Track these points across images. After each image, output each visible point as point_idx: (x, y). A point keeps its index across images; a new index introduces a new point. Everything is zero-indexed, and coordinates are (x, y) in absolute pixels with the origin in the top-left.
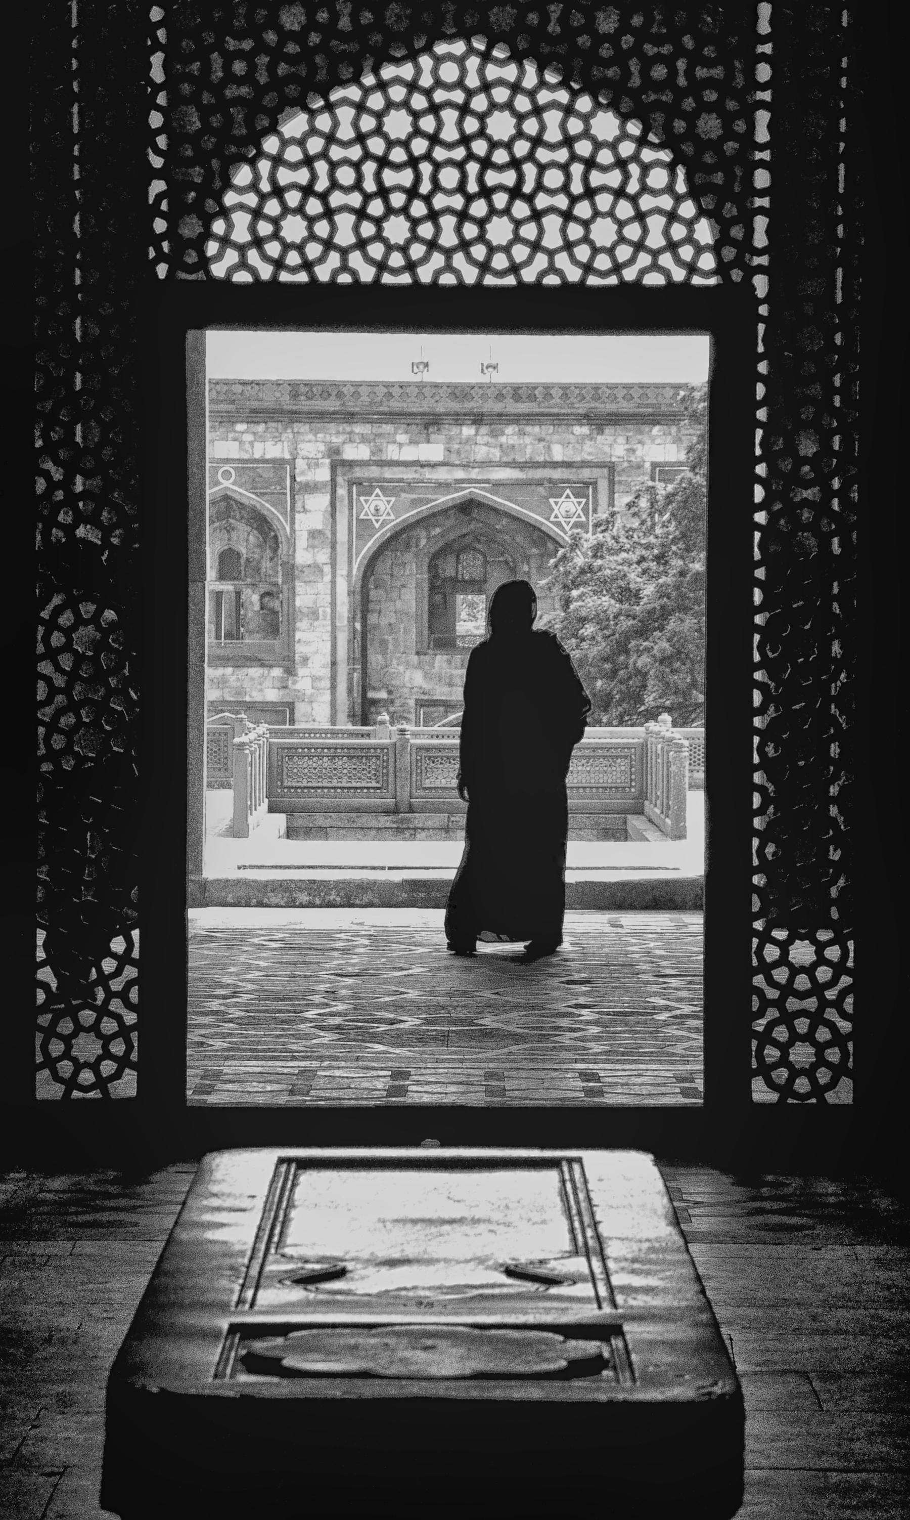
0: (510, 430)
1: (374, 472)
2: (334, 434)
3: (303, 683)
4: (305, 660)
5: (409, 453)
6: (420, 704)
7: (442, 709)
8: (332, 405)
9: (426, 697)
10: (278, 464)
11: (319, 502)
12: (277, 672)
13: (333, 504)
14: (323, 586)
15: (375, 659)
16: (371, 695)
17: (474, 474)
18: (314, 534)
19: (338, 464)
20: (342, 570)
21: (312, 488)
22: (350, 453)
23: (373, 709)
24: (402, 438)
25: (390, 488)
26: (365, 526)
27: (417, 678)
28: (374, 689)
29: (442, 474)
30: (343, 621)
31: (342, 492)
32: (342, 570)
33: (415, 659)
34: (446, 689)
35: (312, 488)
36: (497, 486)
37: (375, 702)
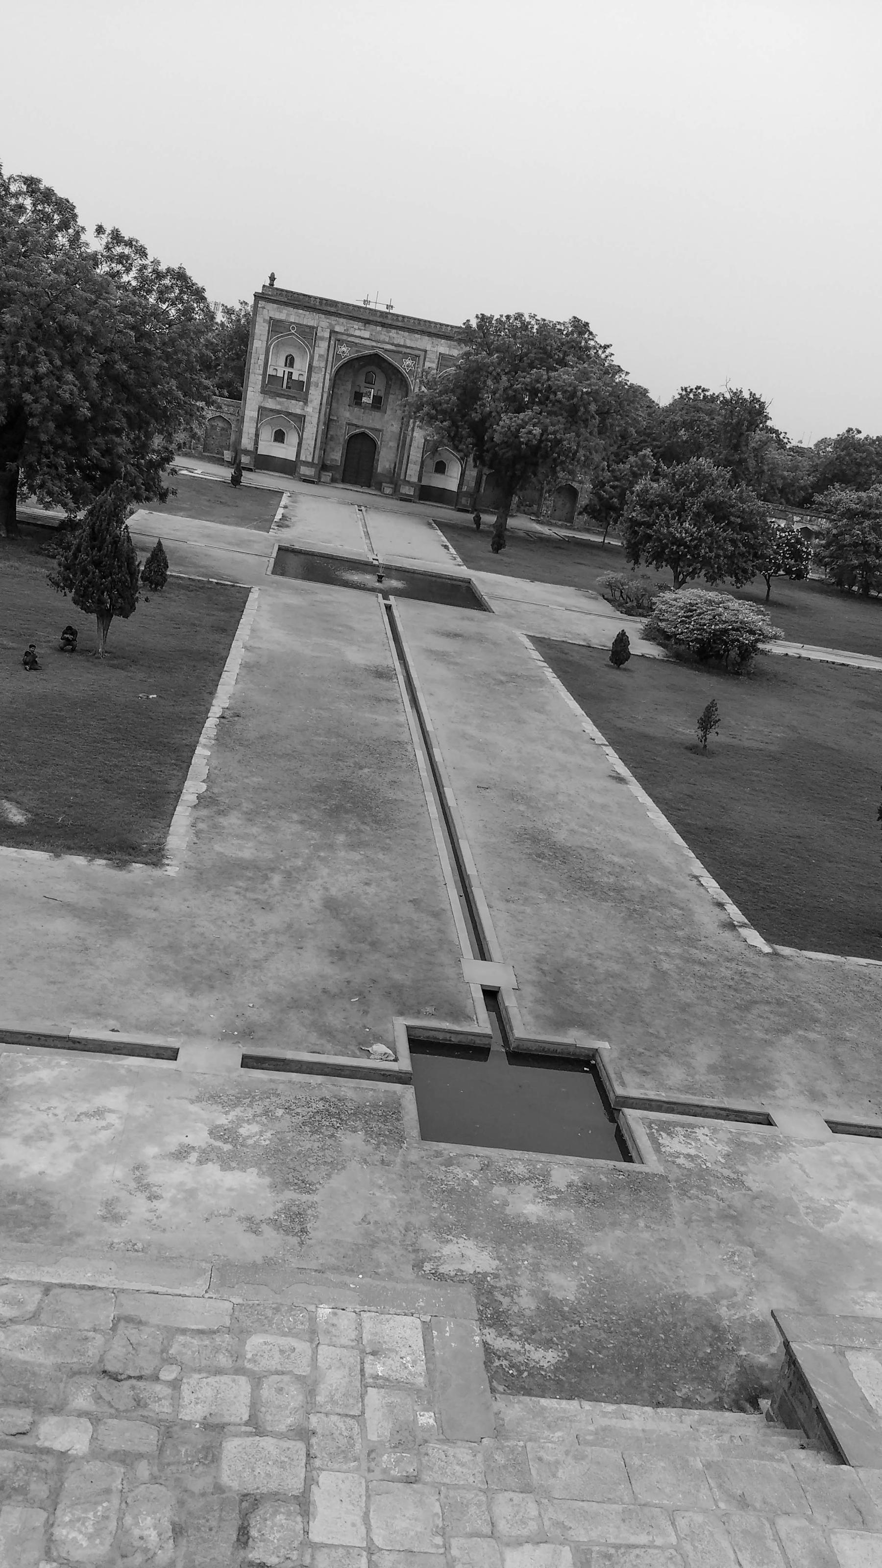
0: (394, 331)
1: (345, 337)
2: (333, 320)
3: (309, 409)
4: (311, 401)
5: (357, 333)
6: (349, 424)
8: (333, 309)
10: (313, 327)
11: (324, 345)
12: (301, 403)
13: (329, 347)
14: (321, 375)
15: (334, 405)
17: (379, 345)
18: (320, 356)
19: (332, 332)
20: (328, 371)
21: (322, 339)
22: (337, 329)
24: (356, 327)
25: (350, 344)
26: (338, 357)
27: (347, 414)
29: (368, 343)
30: (326, 390)
31: (332, 342)
32: (328, 371)
35: (322, 339)
36: (386, 350)
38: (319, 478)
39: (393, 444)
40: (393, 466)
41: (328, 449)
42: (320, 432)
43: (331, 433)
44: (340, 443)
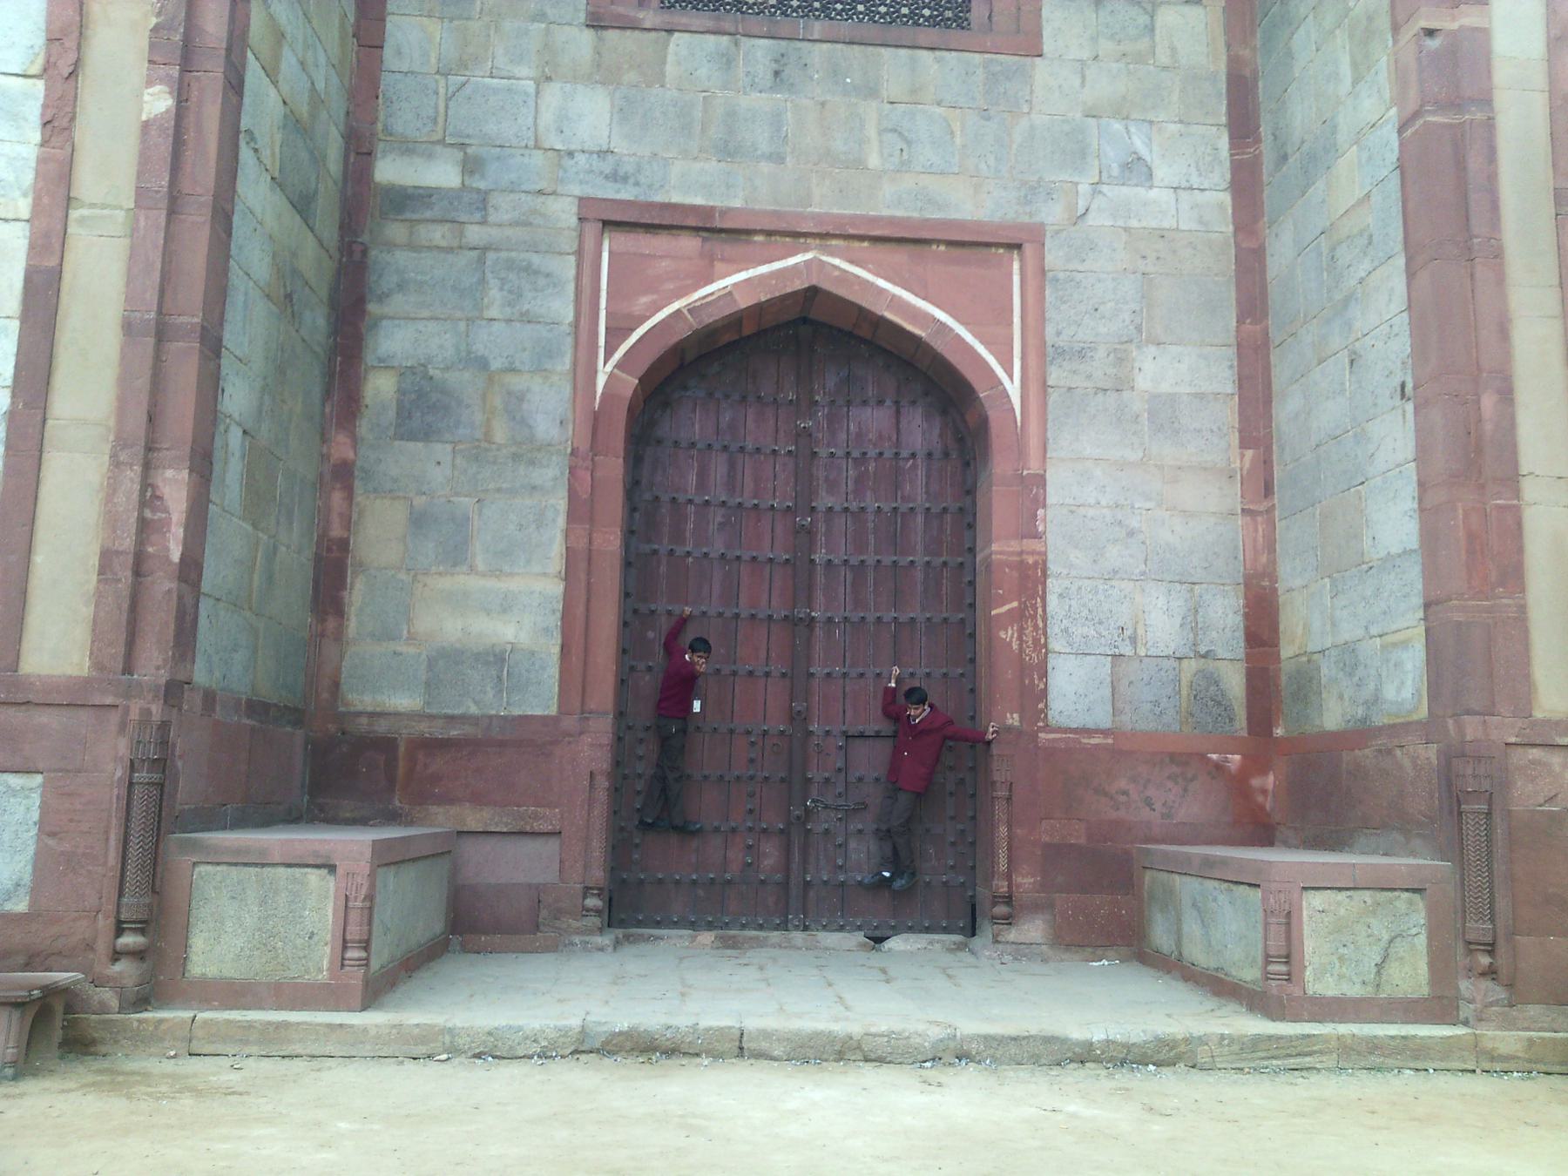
7: (689, 244)
9: (627, 193)
16: (389, 170)
23: (396, 231)
27: (588, 116)
28: (408, 147)
33: (580, 42)
34: (711, 167)
37: (404, 200)
38: (152, 924)
39: (1187, 369)
40: (1225, 615)
41: (380, 533)
42: (110, 174)
43: (400, 340)
44: (527, 451)
